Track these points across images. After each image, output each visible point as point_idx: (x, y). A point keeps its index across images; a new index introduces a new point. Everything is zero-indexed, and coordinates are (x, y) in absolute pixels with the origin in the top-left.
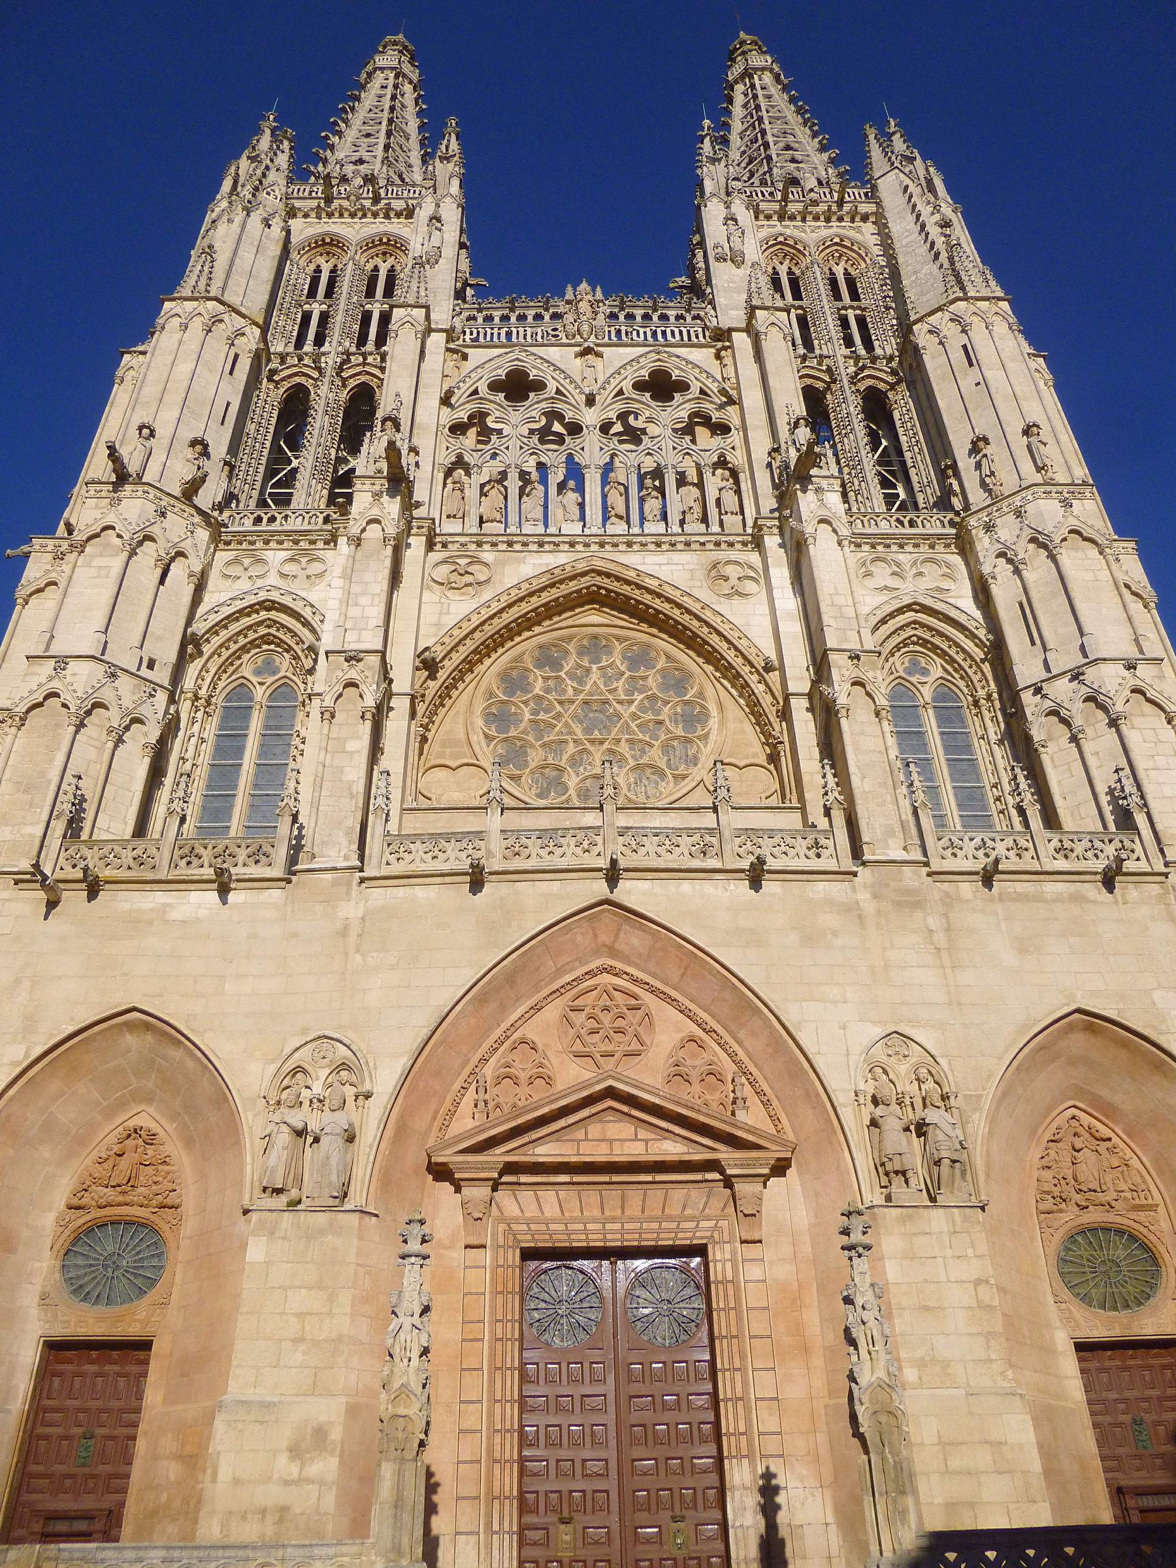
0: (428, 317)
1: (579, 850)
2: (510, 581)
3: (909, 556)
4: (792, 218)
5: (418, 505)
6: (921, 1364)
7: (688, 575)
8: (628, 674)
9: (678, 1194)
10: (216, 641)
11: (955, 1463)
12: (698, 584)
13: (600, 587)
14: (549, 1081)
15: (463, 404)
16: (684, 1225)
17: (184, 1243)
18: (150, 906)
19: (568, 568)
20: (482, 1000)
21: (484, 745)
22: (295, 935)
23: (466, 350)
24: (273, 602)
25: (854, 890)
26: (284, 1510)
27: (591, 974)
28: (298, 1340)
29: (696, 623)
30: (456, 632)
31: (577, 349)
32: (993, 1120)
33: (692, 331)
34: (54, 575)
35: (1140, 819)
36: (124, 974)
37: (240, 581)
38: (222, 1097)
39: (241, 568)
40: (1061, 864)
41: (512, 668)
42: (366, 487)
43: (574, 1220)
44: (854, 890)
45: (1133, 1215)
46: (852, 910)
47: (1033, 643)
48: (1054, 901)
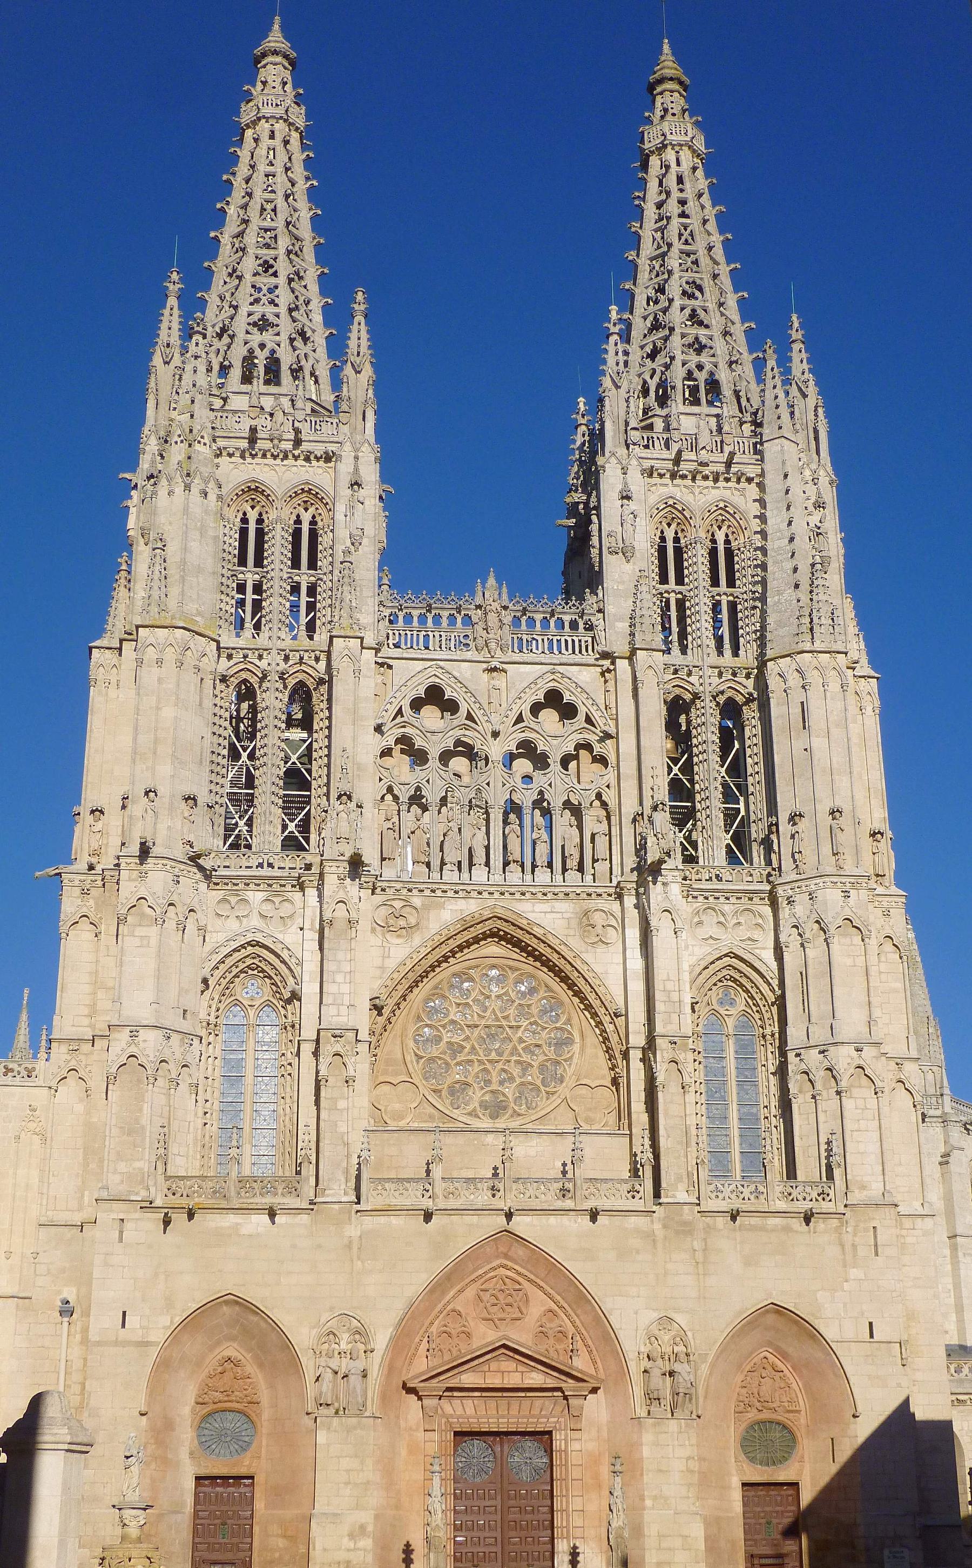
0: (362, 643)
3: (732, 907)
4: (684, 477)
5: (367, 865)
6: (655, 1498)
7: (565, 922)
9: (538, 1403)
11: (664, 1545)
12: (572, 933)
13: (499, 930)
14: (469, 1335)
16: (541, 1420)
17: (265, 1424)
18: (227, 1224)
19: (477, 915)
20: (432, 1291)
21: (415, 1063)
22: (319, 1246)
23: (390, 662)
24: (258, 942)
25: (652, 1222)
26: (348, 1562)
27: (494, 1269)
28: (347, 1483)
29: (568, 967)
31: (485, 666)
32: (713, 1366)
33: (583, 639)
34: (84, 911)
35: (837, 1173)
36: (220, 1271)
37: (229, 920)
38: (286, 1345)
39: (228, 906)
40: (781, 1205)
42: (334, 869)
44: (652, 1222)
45: (786, 1415)
46: (650, 1236)
48: (773, 1230)
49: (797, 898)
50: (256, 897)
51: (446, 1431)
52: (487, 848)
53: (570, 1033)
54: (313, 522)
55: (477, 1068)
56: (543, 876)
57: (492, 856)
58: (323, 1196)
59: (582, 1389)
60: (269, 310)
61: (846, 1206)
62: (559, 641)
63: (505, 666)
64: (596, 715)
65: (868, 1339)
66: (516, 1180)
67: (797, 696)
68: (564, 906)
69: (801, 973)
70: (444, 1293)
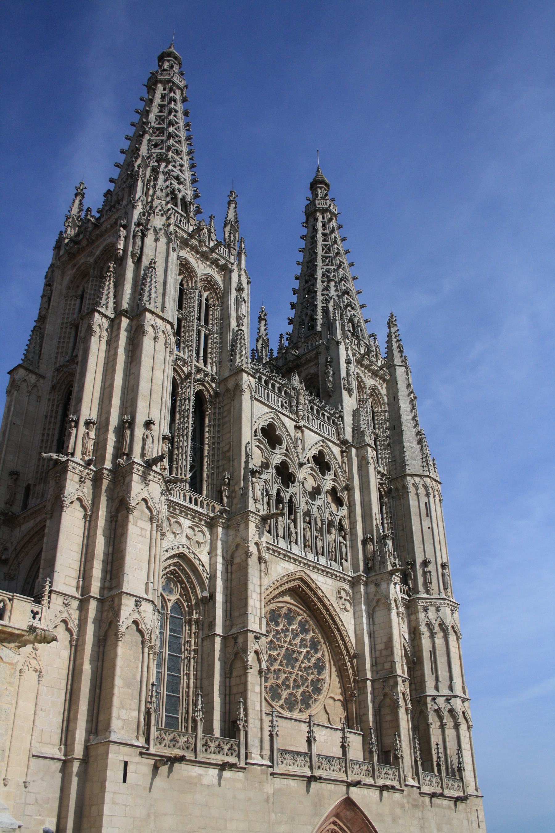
18: (194, 774)
31: (295, 424)
34: (81, 494)
36: (190, 815)
46: (402, 806)
47: (433, 674)
48: (445, 808)
49: (429, 608)
50: (186, 523)
52: (296, 533)
53: (324, 662)
54: (207, 300)
55: (284, 676)
56: (323, 560)
58: (251, 758)
60: (181, 174)
64: (340, 474)
67: (423, 499)
68: (330, 581)
69: (430, 651)
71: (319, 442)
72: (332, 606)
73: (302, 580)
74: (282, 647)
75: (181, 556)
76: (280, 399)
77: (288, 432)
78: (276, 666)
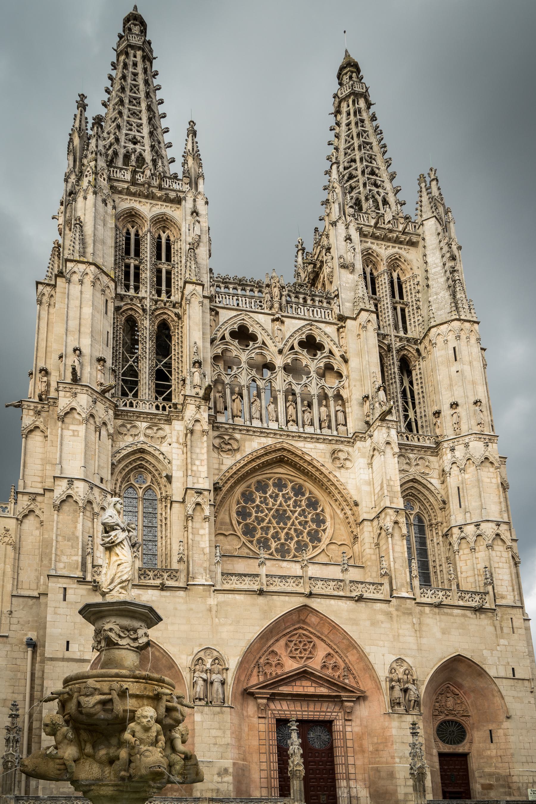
1: (294, 585)
2: (248, 451)
8: (294, 498)
10: (121, 466)
12: (327, 460)
15: (219, 345)
19: (273, 447)
30: (227, 474)
31: (272, 317)
33: (326, 311)
37: (126, 437)
39: (125, 429)
40: (461, 603)
41: (246, 491)
43: (293, 711)
48: (456, 616)
49: (456, 447)
51: (271, 718)
56: (309, 429)
57: (279, 416)
59: (352, 697)
61: (496, 606)
62: (313, 311)
63: (284, 319)
64: (335, 350)
65: (512, 676)
66: (310, 578)
70: (268, 640)
71: (303, 326)
72: (323, 466)
73: (284, 449)
74: (270, 510)
75: (142, 451)
76: (253, 300)
77: (261, 326)
78: (264, 524)
